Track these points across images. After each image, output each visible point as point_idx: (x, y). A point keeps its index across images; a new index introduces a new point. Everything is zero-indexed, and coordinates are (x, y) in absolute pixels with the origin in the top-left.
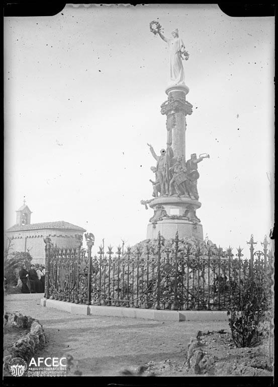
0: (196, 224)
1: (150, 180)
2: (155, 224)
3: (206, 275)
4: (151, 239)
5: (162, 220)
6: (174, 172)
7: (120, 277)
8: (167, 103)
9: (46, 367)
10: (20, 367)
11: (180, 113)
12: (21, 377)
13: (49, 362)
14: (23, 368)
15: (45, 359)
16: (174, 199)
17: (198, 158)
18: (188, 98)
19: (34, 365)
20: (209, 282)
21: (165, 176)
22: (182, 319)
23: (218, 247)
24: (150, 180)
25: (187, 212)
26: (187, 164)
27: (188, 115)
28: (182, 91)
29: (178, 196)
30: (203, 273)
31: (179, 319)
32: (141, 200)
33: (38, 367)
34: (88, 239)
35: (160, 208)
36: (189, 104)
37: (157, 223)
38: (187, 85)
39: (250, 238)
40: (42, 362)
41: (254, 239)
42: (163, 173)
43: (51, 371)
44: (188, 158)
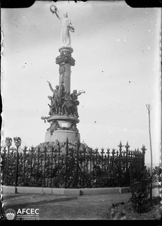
0: (77, 134)
1: (48, 104)
2: (52, 132)
3: (89, 165)
4: (49, 141)
5: (57, 129)
6: (64, 101)
7: (32, 166)
8: (59, 57)
9: (27, 214)
10: (12, 214)
11: (68, 64)
12: (12, 220)
13: (29, 211)
14: (13, 215)
15: (26, 210)
16: (65, 117)
17: (78, 93)
18: (73, 55)
19: (20, 213)
20: (90, 169)
21: (59, 102)
22: (81, 194)
23: (90, 148)
24: (48, 104)
25: (72, 125)
26: (72, 95)
27: (72, 66)
28: (70, 51)
29: (68, 116)
30: (87, 164)
31: (79, 194)
32: (41, 116)
33: (22, 214)
34: (16, 141)
35: (55, 122)
36: (73, 59)
37: (53, 132)
38: (72, 46)
39: (126, 143)
40: (25, 211)
41: (122, 144)
42: (58, 100)
43: (30, 216)
44: (71, 92)
